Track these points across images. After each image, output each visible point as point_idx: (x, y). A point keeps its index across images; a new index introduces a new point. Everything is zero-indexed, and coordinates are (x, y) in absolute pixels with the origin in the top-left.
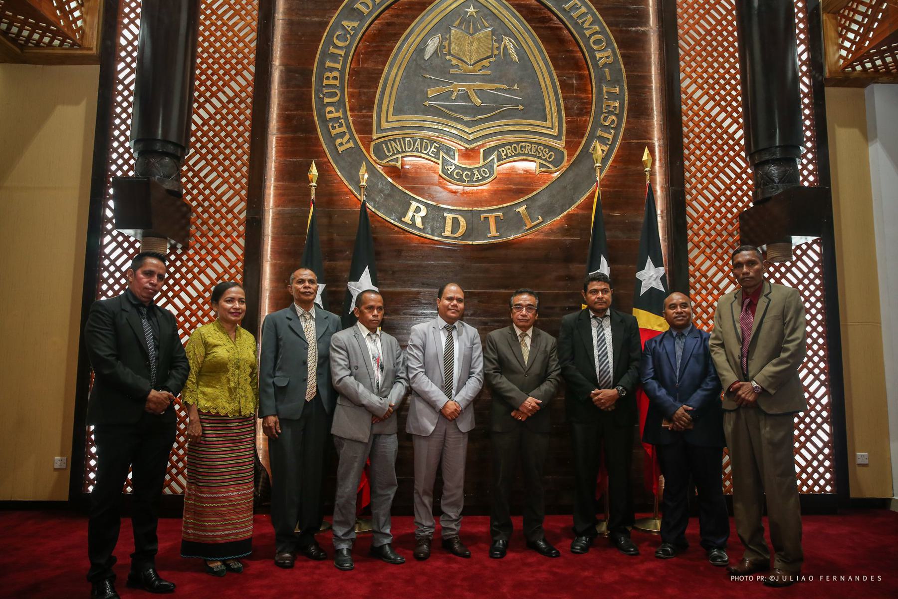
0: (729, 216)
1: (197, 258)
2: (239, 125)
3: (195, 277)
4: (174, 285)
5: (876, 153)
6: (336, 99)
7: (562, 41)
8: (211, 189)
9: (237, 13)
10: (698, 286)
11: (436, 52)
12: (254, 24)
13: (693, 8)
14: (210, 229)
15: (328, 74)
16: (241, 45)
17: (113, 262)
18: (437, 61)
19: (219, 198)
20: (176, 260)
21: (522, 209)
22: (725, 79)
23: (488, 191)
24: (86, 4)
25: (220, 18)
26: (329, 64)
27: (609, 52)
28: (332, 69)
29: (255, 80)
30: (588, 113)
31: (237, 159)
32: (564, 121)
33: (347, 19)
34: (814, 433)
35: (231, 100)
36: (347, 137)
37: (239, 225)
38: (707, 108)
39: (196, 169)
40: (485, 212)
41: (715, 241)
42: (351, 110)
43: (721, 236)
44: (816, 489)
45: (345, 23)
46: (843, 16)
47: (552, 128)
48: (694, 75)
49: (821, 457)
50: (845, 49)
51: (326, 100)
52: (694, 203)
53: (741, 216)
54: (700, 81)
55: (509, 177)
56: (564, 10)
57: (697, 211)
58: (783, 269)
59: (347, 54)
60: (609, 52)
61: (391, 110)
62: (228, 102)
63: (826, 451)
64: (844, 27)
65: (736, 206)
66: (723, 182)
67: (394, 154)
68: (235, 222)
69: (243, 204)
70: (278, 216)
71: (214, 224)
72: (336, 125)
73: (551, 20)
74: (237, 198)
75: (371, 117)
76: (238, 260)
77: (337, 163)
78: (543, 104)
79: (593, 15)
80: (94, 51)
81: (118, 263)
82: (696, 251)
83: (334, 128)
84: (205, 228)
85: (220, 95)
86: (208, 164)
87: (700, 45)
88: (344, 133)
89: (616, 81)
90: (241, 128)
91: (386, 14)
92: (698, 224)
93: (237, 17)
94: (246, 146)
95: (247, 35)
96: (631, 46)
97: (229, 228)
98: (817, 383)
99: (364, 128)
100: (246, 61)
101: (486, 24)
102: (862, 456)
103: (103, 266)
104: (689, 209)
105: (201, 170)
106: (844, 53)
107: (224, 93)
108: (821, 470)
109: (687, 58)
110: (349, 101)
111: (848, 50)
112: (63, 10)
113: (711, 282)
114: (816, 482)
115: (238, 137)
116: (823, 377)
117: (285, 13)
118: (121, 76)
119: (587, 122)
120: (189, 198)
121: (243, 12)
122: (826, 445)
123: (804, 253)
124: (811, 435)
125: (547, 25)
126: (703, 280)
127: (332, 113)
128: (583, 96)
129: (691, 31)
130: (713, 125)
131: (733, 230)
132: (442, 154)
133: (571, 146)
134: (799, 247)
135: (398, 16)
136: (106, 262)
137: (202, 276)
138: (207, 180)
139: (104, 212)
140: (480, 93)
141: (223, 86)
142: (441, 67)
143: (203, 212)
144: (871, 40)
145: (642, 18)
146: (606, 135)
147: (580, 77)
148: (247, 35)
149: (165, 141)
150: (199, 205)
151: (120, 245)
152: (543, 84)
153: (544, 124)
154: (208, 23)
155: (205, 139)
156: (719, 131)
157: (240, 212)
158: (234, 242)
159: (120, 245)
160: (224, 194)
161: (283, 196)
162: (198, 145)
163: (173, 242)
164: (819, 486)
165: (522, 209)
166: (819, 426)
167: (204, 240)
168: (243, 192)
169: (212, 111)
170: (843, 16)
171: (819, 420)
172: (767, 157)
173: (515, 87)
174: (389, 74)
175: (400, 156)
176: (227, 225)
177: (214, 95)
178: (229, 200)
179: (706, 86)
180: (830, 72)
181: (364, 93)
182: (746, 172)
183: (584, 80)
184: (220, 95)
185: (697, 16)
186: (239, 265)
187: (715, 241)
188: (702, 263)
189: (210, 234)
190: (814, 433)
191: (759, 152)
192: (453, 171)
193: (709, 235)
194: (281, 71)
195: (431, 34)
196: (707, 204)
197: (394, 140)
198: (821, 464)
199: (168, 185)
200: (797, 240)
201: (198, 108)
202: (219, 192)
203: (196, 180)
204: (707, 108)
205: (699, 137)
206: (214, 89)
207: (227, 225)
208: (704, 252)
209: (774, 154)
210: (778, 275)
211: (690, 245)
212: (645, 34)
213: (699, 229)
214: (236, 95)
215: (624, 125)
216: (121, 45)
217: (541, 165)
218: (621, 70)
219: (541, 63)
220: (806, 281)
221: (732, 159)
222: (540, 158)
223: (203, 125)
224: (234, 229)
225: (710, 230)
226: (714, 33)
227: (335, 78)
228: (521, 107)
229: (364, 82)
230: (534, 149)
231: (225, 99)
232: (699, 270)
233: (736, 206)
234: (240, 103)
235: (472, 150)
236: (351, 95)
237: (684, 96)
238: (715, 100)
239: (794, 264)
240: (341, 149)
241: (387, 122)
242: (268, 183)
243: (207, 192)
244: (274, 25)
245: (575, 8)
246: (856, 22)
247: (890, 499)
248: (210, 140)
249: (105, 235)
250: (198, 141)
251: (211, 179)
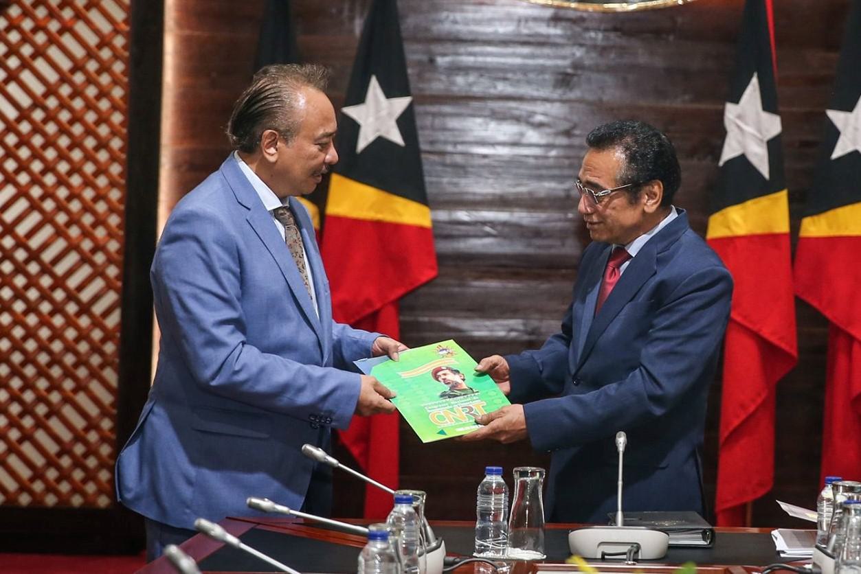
1: (27, 25)
3: (25, 64)
76: (116, 31)
137: (40, 64)
186: (119, 41)
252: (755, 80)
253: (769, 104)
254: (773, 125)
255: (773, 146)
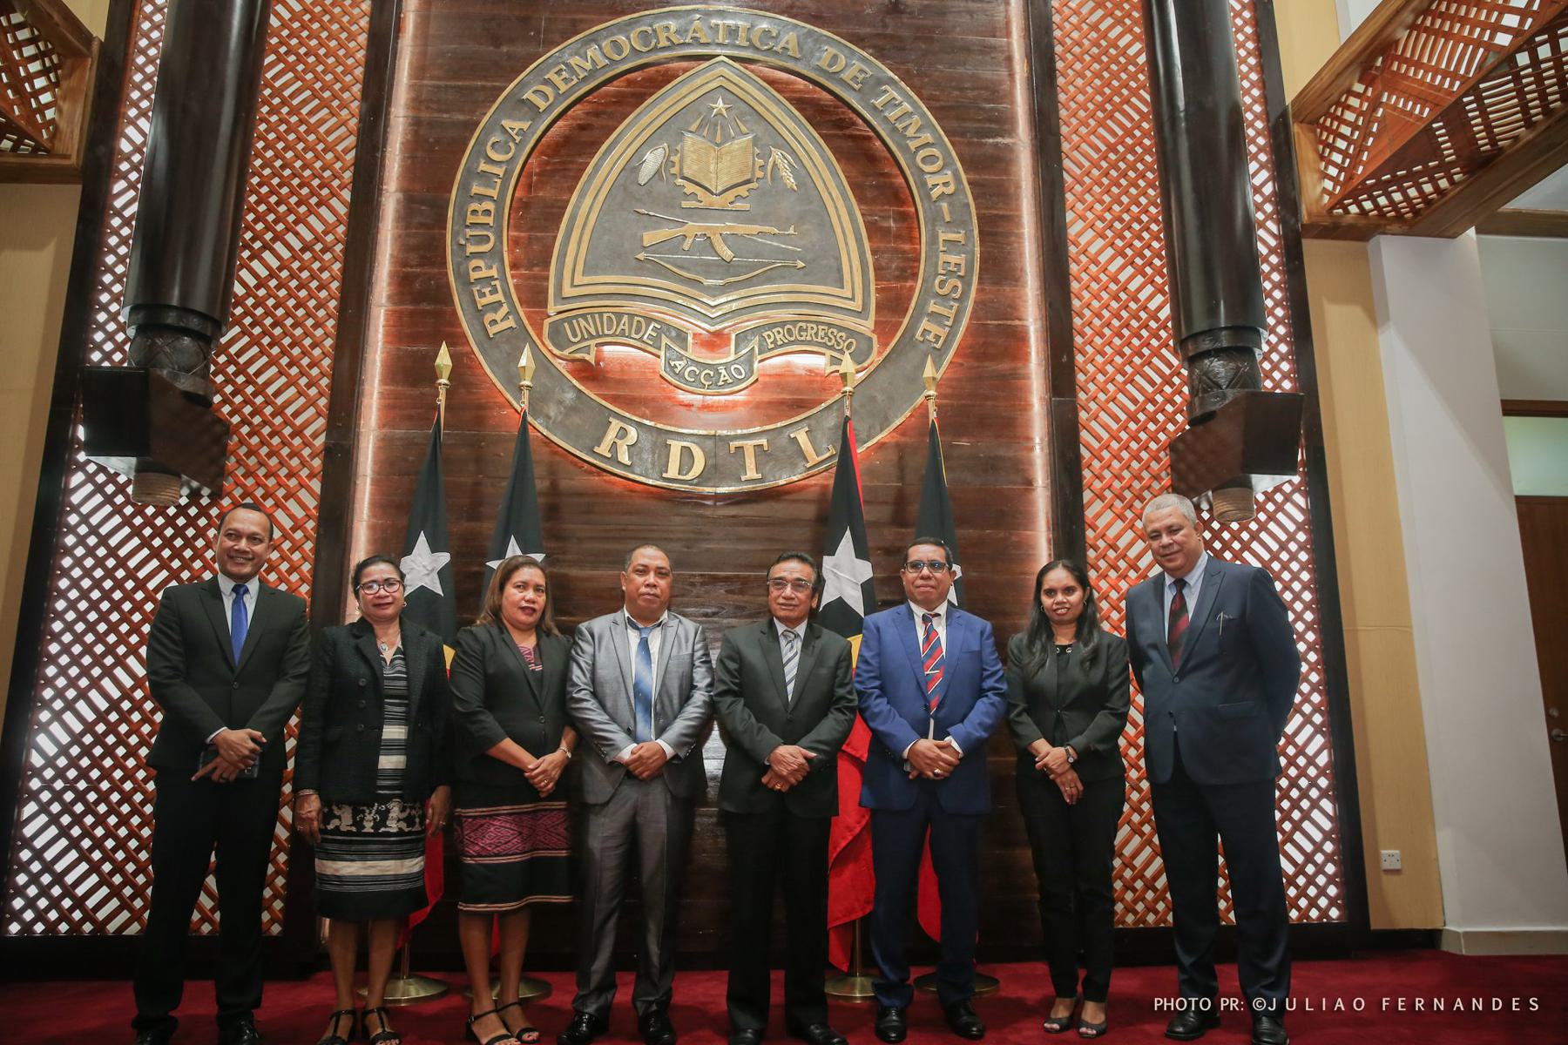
0: (1153, 446)
2: (319, 288)
4: (193, 559)
5: (1391, 345)
6: (486, 248)
7: (872, 158)
8: (266, 396)
9: (325, 104)
10: (1102, 564)
11: (658, 172)
12: (353, 122)
13: (1086, 109)
14: (261, 464)
15: (474, 206)
16: (329, 156)
17: (85, 519)
18: (661, 187)
19: (279, 411)
20: (198, 516)
21: (802, 437)
22: (1140, 222)
23: (746, 403)
24: (65, 84)
25: (294, 111)
26: (476, 189)
27: (948, 176)
28: (481, 198)
29: (350, 215)
30: (915, 276)
31: (313, 346)
32: (873, 287)
33: (510, 117)
34: (1306, 816)
35: (307, 247)
36: (505, 309)
37: (312, 456)
38: (1113, 268)
39: (242, 360)
40: (736, 437)
41: (1129, 487)
42: (514, 266)
43: (1140, 479)
44: (1314, 913)
45: (506, 123)
46: (1324, 128)
47: (853, 299)
48: (1089, 215)
49: (1319, 858)
50: (1331, 178)
51: (471, 249)
52: (1094, 424)
53: (1172, 447)
54: (1099, 224)
55: (781, 380)
56: (875, 108)
57: (1098, 438)
58: (1245, 536)
59: (508, 174)
60: (948, 176)
61: (580, 268)
62: (303, 250)
63: (1329, 847)
64: (1326, 145)
65: (1164, 430)
66: (1141, 390)
67: (583, 339)
68: (306, 452)
69: (321, 421)
70: (386, 444)
71: (269, 455)
72: (487, 290)
73: (854, 124)
74: (312, 411)
75: (547, 278)
76: (308, 517)
77: (484, 353)
78: (838, 259)
79: (923, 115)
80: (73, 161)
81: (94, 520)
82: (1098, 505)
83: (483, 295)
84: (252, 461)
85: (290, 237)
86: (262, 352)
87: (1100, 168)
88: (500, 303)
89: (957, 223)
90: (323, 294)
91: (578, 110)
92: (1101, 459)
93: (325, 111)
94: (331, 323)
95: (341, 139)
96: (986, 171)
97: (295, 462)
98: (1309, 730)
99: (535, 297)
100: (336, 183)
101: (744, 129)
102: (1390, 856)
103: (68, 525)
104: (1084, 434)
105: (250, 362)
106: (1329, 185)
107: (296, 234)
108: (1321, 880)
109: (1078, 188)
110: (511, 251)
111: (1335, 180)
112: (19, 91)
113: (1124, 557)
114: (1313, 903)
115: (317, 308)
116: (1318, 719)
117: (408, 107)
118: (118, 203)
119: (912, 289)
120: (226, 409)
121: (335, 103)
122: (1327, 836)
123: (1280, 508)
124: (1302, 820)
125: (847, 132)
126: (1111, 554)
127: (482, 270)
128: (907, 247)
129: (1084, 146)
130: (1123, 296)
131: (1160, 470)
132: (665, 340)
133: (884, 329)
134: (1269, 497)
135: (597, 114)
136: (73, 519)
138: (261, 380)
139: (75, 431)
140: (731, 239)
141: (296, 222)
142: (667, 195)
143: (250, 435)
144: (1366, 164)
145: (1004, 124)
146: (944, 311)
147: (903, 217)
148: (341, 139)
149: (184, 310)
150: (244, 422)
151: (99, 489)
152: (838, 230)
153: (837, 291)
154: (274, 118)
155: (259, 311)
156: (1133, 305)
157: (315, 435)
158: (301, 485)
159: (99, 489)
160: (288, 403)
161: (393, 409)
162: (248, 321)
163: (195, 484)
164: (1319, 908)
165: (802, 437)
166: (1315, 804)
167: (250, 482)
168: (323, 402)
169: (275, 263)
170: (1324, 128)
171: (1314, 793)
172: (1206, 345)
173: (791, 231)
174: (577, 206)
175: (593, 343)
176: (291, 456)
177: (278, 237)
178: (296, 414)
179: (1109, 233)
180: (1309, 215)
181: (538, 239)
182: (1179, 374)
183: (909, 222)
184: (290, 237)
185: (1092, 122)
186: (311, 525)
187: (1129, 487)
188: (1109, 526)
189: (262, 472)
190: (1306, 816)
191: (1194, 337)
192: (684, 368)
193: (1119, 477)
194: (398, 201)
195: (649, 143)
196: (1114, 426)
197: (584, 316)
198: (1320, 870)
199: (185, 384)
200: (1263, 483)
201: (251, 258)
202: (280, 401)
203: (241, 379)
204: (1113, 268)
205: (1100, 316)
206: (280, 227)
207: (291, 456)
208: (1111, 507)
209: (1217, 340)
210: (1236, 545)
211: (1087, 496)
212: (1009, 149)
213: (1102, 468)
214: (317, 239)
215: (973, 294)
216: (121, 152)
217: (835, 361)
218: (967, 205)
219: (835, 193)
220: (1284, 556)
221: (1156, 353)
222: (831, 348)
223: (258, 287)
224: (303, 464)
225: (1122, 469)
226: (1121, 148)
227: (487, 212)
228: (801, 264)
229: (537, 216)
230: (821, 334)
231: (297, 245)
232: (1103, 536)
233: (1164, 430)
234: (324, 251)
235: (718, 334)
236: (515, 242)
237: (1072, 250)
238: (1124, 255)
239: (1263, 527)
240: (492, 330)
241: (573, 286)
242: (367, 387)
243: (259, 400)
244: (387, 125)
245: (891, 104)
246: (1343, 137)
247: (1439, 932)
248: (268, 313)
249: (75, 471)
250: (247, 313)
251: (267, 376)
252: (848, 533)
253: (861, 552)
254: (865, 570)
255: (867, 588)
